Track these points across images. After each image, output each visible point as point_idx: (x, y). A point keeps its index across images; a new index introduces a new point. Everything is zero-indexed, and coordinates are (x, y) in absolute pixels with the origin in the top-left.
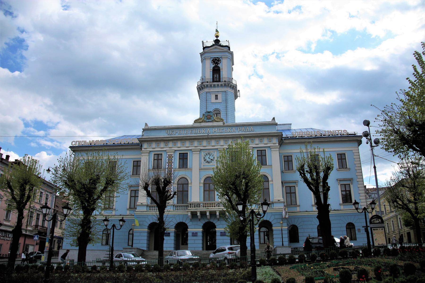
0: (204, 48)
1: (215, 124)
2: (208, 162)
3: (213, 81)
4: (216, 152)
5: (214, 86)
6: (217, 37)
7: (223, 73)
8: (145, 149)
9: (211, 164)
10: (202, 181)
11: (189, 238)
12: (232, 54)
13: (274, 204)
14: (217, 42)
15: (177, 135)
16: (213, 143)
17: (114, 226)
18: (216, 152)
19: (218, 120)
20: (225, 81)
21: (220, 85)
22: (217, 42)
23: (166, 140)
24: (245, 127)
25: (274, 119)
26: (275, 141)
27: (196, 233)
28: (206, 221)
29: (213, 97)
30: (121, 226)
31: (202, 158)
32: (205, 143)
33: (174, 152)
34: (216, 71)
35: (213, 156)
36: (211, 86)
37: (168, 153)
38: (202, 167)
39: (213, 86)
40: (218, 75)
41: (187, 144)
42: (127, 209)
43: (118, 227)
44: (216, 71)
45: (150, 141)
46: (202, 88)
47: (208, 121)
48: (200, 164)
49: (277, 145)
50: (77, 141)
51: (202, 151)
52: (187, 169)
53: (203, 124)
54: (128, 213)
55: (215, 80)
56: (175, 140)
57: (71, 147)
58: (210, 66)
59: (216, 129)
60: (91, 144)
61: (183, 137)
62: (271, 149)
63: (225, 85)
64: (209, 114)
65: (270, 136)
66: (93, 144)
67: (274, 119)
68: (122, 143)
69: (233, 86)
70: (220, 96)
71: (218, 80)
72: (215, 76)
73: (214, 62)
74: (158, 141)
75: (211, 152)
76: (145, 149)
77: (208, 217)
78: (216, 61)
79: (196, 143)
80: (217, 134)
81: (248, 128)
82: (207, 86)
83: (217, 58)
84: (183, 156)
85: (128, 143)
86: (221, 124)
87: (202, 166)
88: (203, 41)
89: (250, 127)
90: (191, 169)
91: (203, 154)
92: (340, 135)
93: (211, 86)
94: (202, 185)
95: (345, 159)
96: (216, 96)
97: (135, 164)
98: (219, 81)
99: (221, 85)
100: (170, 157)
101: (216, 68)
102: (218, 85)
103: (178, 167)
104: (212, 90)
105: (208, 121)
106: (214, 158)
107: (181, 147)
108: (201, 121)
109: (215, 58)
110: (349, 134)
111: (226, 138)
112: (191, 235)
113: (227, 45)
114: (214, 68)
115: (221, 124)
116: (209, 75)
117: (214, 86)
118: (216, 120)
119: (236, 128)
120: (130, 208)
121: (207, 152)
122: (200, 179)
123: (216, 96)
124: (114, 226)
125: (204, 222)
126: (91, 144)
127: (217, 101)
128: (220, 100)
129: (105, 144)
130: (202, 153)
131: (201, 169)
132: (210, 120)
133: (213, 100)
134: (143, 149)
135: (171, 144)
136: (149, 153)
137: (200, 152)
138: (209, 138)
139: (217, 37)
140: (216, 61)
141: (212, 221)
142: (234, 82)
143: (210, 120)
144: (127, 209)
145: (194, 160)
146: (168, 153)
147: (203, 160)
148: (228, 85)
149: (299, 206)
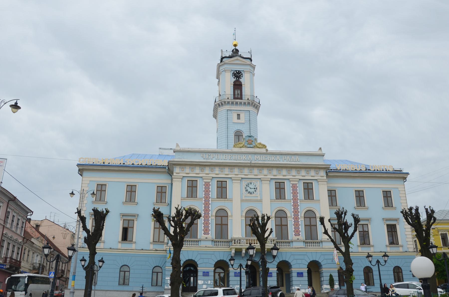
0: (222, 58)
2: (249, 192)
3: (235, 98)
4: (258, 182)
5: (237, 103)
7: (246, 89)
8: (177, 173)
9: (253, 195)
10: (244, 214)
11: (231, 278)
12: (254, 67)
13: (323, 243)
14: (236, 52)
15: (214, 160)
16: (256, 171)
17: (378, 262)
18: (258, 182)
19: (260, 146)
20: (248, 99)
21: (243, 103)
22: (236, 52)
23: (202, 165)
24: (290, 156)
25: (320, 149)
26: (323, 173)
27: (208, 272)
29: (235, 116)
30: (385, 261)
31: (244, 188)
32: (246, 171)
33: (211, 180)
34: (238, 86)
36: (232, 103)
37: (205, 181)
38: (244, 198)
39: (234, 103)
40: (239, 91)
41: (227, 170)
42: (151, 243)
43: (382, 261)
46: (222, 104)
47: (249, 146)
48: (241, 194)
49: (325, 178)
50: (86, 158)
51: (243, 180)
52: (226, 200)
53: (244, 150)
54: (151, 247)
55: (236, 96)
56: (212, 166)
57: (78, 165)
59: (259, 156)
60: (104, 163)
61: (223, 163)
62: (318, 182)
63: (249, 103)
64: (250, 138)
65: (317, 168)
66: (106, 164)
67: (320, 149)
68: (144, 164)
69: (257, 105)
70: (242, 116)
71: (239, 96)
72: (236, 92)
73: (235, 76)
74: (193, 165)
75: (253, 181)
76: (177, 173)
78: (237, 75)
79: (236, 171)
80: (260, 162)
81: (293, 157)
82: (228, 103)
83: (239, 71)
85: (151, 165)
86: (263, 150)
87: (244, 197)
88: (222, 51)
89: (295, 156)
90: (231, 200)
91: (244, 183)
92: (385, 171)
93: (232, 103)
94: (244, 218)
95: (391, 197)
96: (239, 115)
97: (129, 189)
98: (241, 98)
99: (245, 103)
100: (207, 185)
102: (241, 103)
103: (216, 197)
104: (234, 108)
105: (249, 146)
106: (256, 188)
108: (241, 145)
109: (236, 71)
110: (395, 171)
112: (304, 273)
113: (250, 57)
115: (263, 150)
116: (229, 90)
117: (237, 103)
118: (258, 145)
119: (281, 156)
120: (154, 242)
121: (249, 181)
122: (242, 211)
123: (239, 115)
124: (378, 262)
126: (104, 163)
128: (242, 120)
129: (122, 164)
130: (244, 182)
131: (242, 201)
132: (251, 146)
134: (174, 174)
135: (207, 170)
136: (182, 179)
137: (241, 180)
138: (251, 166)
140: (237, 75)
143: (251, 146)
144: (151, 243)
145: (235, 190)
146: (205, 181)
147: (244, 190)
148: (252, 104)
149: (373, 246)
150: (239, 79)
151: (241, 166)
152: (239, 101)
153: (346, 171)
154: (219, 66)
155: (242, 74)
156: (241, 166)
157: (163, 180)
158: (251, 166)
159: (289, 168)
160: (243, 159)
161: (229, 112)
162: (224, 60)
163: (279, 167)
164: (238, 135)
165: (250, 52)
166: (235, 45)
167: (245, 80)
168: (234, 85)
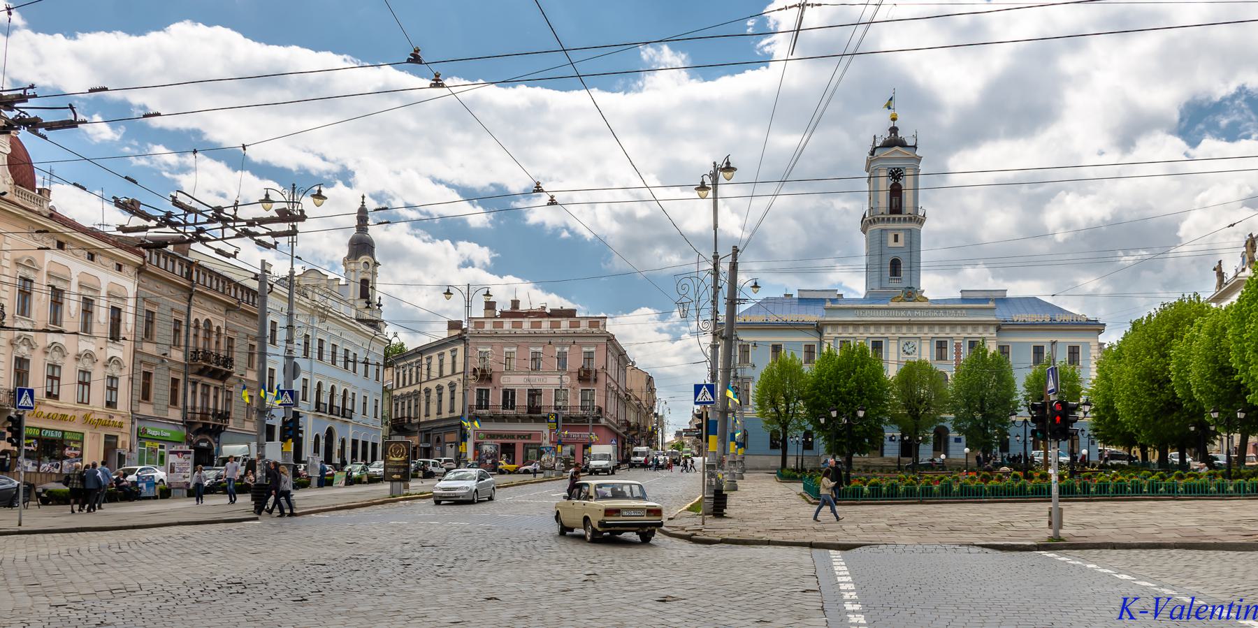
1: (917, 304)
3: (892, 211)
6: (894, 120)
14: (894, 130)
16: (915, 329)
22: (894, 130)
26: (992, 330)
32: (904, 329)
34: (896, 191)
41: (883, 329)
44: (896, 191)
45: (835, 325)
53: (903, 304)
58: (885, 183)
63: (910, 219)
65: (986, 325)
70: (901, 236)
78: (896, 175)
79: (893, 329)
91: (902, 343)
96: (896, 236)
107: (875, 334)
111: (931, 325)
116: (884, 201)
123: (896, 236)
127: (897, 245)
128: (901, 243)
133: (891, 243)
138: (910, 324)
139: (894, 120)
140: (896, 175)
142: (921, 213)
151: (899, 324)
152: (897, 216)
153: (1025, 323)
154: (869, 162)
156: (899, 324)
157: (812, 339)
158: (910, 324)
159: (953, 325)
163: (942, 325)
164: (895, 266)
167: (907, 182)
168: (892, 191)
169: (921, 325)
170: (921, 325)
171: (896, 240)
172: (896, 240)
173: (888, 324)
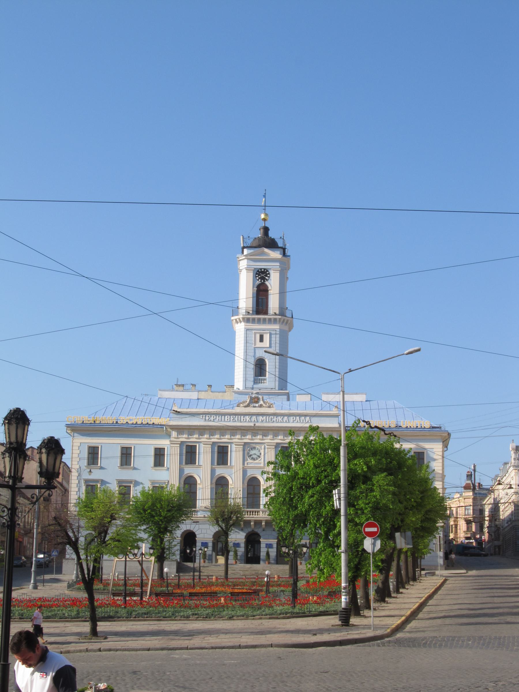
5: (259, 320)
9: (257, 461)
21: (267, 320)
28: (250, 530)
35: (259, 451)
60: (95, 422)
70: (266, 337)
75: (257, 446)
77: (253, 527)
78: (262, 275)
83: (265, 269)
84: (223, 448)
93: (254, 319)
99: (270, 320)
101: (262, 288)
102: (264, 320)
104: (256, 326)
106: (260, 454)
109: (261, 269)
114: (258, 287)
125: (247, 532)
126: (95, 422)
132: (257, 405)
140: (262, 275)
141: (256, 530)
150: (264, 281)
152: (262, 317)
155: (269, 274)
158: (254, 431)
160: (247, 422)
161: (248, 332)
162: (246, 251)
165: (282, 238)
166: (264, 220)
169: (265, 431)
170: (265, 431)
171: (261, 340)
172: (261, 340)
173: (234, 430)
